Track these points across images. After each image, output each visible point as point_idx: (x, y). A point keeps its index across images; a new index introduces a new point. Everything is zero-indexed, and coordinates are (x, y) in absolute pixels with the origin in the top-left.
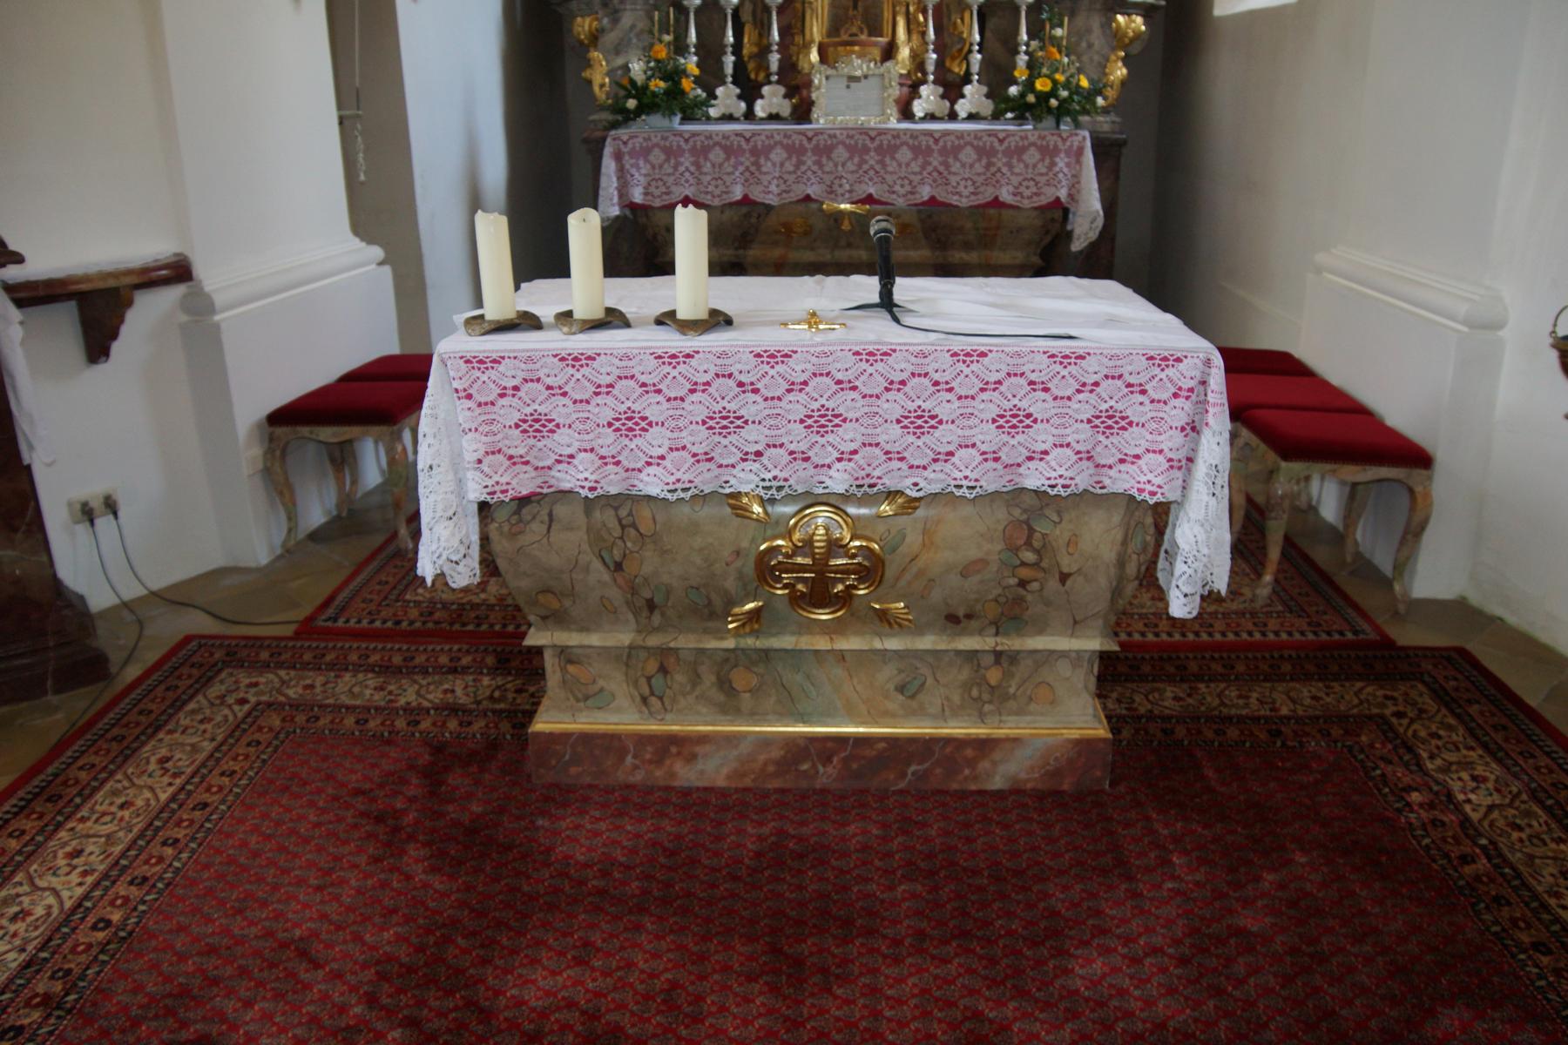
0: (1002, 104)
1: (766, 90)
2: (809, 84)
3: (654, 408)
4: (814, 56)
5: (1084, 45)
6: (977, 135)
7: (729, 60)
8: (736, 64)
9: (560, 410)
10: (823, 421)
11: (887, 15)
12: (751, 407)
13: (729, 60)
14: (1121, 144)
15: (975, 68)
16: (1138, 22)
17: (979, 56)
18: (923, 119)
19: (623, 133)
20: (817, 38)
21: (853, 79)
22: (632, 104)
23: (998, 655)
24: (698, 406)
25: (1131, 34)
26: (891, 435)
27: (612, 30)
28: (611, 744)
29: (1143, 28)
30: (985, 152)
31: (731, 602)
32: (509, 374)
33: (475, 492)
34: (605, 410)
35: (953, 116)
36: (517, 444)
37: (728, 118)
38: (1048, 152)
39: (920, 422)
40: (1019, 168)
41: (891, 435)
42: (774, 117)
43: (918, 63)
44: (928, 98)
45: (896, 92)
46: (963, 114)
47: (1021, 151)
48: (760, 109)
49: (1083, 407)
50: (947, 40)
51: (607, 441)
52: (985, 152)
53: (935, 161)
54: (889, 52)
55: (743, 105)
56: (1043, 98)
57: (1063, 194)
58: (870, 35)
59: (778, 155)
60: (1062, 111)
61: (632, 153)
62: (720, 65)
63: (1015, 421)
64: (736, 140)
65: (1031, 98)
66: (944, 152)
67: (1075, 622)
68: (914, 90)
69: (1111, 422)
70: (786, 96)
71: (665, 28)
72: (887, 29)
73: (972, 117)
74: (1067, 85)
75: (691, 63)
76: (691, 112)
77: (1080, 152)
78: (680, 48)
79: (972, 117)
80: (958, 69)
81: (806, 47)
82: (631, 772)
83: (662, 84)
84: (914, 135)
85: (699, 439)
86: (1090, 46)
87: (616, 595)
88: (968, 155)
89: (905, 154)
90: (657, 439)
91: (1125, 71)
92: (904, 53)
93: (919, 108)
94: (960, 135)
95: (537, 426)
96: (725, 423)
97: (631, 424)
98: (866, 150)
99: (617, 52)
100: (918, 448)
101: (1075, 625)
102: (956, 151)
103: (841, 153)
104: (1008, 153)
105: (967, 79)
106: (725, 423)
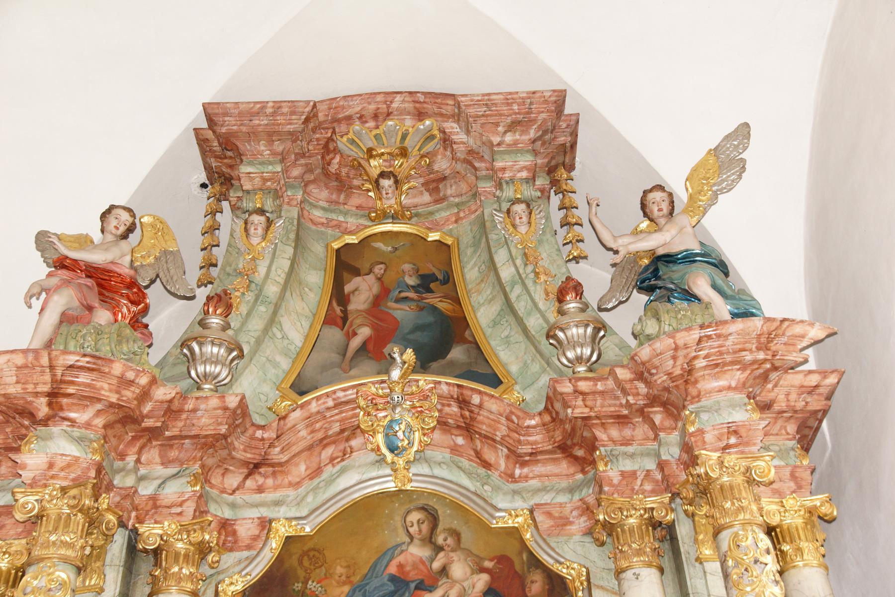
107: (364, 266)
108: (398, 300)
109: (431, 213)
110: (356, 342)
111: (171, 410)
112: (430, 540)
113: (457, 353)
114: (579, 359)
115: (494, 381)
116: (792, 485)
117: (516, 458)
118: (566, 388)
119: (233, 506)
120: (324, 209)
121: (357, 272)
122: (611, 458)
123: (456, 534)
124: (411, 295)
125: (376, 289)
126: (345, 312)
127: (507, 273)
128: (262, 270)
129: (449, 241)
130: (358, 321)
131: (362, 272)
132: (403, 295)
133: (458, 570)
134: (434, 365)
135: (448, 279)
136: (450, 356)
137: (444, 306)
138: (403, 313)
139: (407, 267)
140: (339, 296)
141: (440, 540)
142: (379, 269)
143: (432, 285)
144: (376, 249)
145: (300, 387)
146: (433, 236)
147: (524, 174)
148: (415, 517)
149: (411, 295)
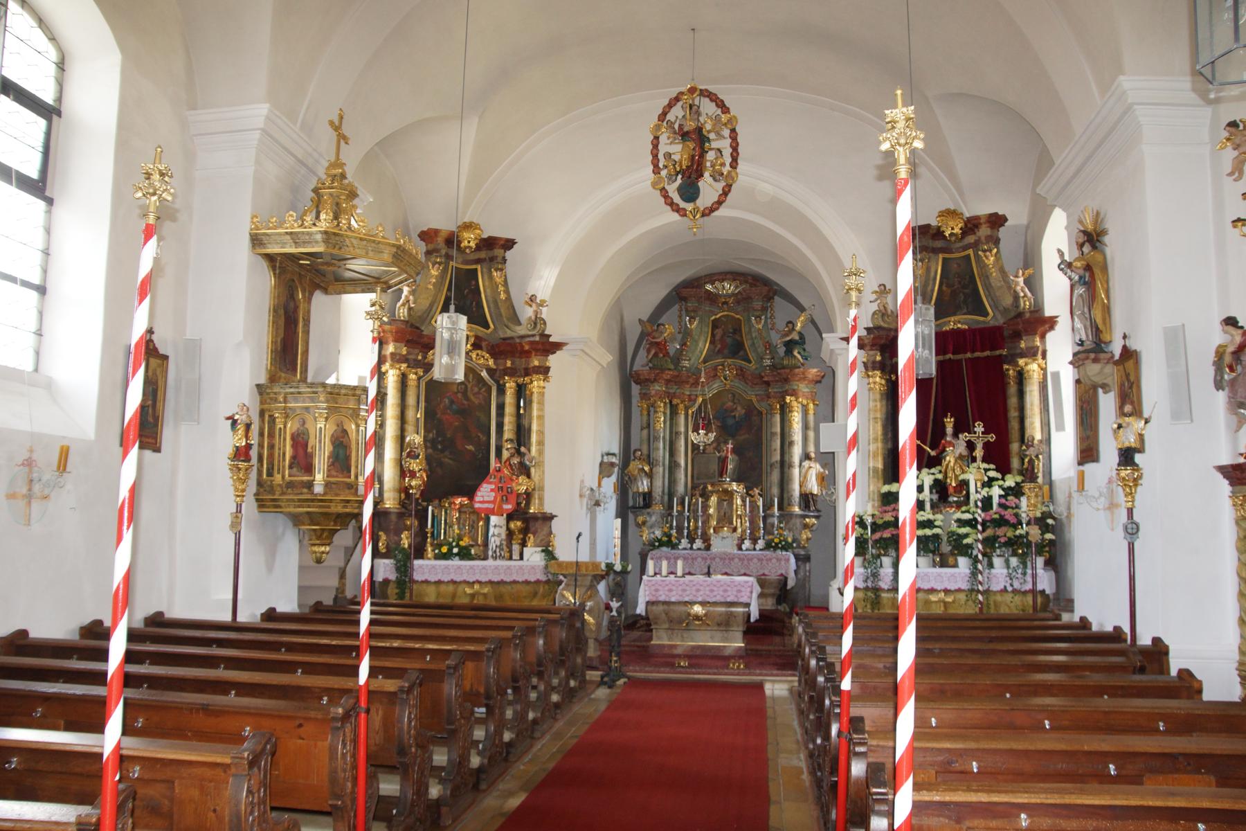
0: (769, 546)
1: (697, 541)
2: (710, 539)
3: (674, 588)
4: (712, 531)
6: (758, 555)
7: (686, 531)
8: (688, 533)
9: (660, 588)
10: (698, 590)
11: (735, 519)
12: (688, 588)
13: (686, 531)
15: (762, 535)
16: (814, 520)
18: (747, 550)
19: (654, 552)
21: (723, 538)
22: (657, 544)
24: (680, 588)
26: (708, 593)
28: (663, 646)
30: (760, 560)
31: (683, 621)
32: (653, 583)
33: (647, 599)
34: (667, 588)
35: (755, 549)
36: (654, 593)
37: (685, 549)
38: (779, 560)
39: (712, 591)
40: (770, 565)
41: (708, 593)
42: (699, 549)
44: (747, 544)
45: (736, 542)
46: (758, 549)
47: (770, 559)
48: (695, 547)
49: (735, 589)
51: (667, 593)
52: (760, 560)
53: (746, 562)
54: (735, 530)
55: (689, 545)
56: (777, 544)
57: (783, 572)
59: (699, 560)
60: (784, 548)
61: (657, 558)
62: (683, 533)
63: (725, 591)
64: (687, 556)
65: (773, 544)
66: (748, 560)
68: (742, 542)
69: (739, 591)
70: (704, 543)
71: (667, 523)
72: (735, 523)
73: (761, 550)
74: (784, 540)
75: (674, 532)
76: (674, 546)
77: (788, 560)
78: (671, 527)
79: (761, 550)
81: (709, 528)
82: (666, 651)
83: (666, 539)
84: (739, 555)
85: (680, 593)
87: (666, 619)
88: (755, 560)
89: (737, 560)
90: (674, 593)
92: (739, 530)
93: (744, 547)
94: (753, 555)
95: (657, 590)
96: (684, 590)
97: (670, 590)
98: (725, 559)
100: (712, 595)
101: (738, 626)
102: (751, 559)
103: (717, 560)
104: (767, 560)
105: (760, 539)
106: (684, 590)
108: (728, 337)
110: (717, 349)
111: (678, 376)
112: (733, 401)
113: (741, 353)
114: (767, 366)
115: (750, 362)
117: (753, 384)
118: (763, 374)
119: (690, 391)
121: (717, 328)
122: (773, 388)
123: (739, 400)
125: (722, 332)
127: (754, 335)
128: (694, 333)
129: (741, 318)
133: (739, 408)
135: (740, 330)
137: (739, 338)
139: (730, 326)
140: (713, 335)
141: (736, 401)
145: (705, 361)
146: (738, 316)
148: (730, 396)
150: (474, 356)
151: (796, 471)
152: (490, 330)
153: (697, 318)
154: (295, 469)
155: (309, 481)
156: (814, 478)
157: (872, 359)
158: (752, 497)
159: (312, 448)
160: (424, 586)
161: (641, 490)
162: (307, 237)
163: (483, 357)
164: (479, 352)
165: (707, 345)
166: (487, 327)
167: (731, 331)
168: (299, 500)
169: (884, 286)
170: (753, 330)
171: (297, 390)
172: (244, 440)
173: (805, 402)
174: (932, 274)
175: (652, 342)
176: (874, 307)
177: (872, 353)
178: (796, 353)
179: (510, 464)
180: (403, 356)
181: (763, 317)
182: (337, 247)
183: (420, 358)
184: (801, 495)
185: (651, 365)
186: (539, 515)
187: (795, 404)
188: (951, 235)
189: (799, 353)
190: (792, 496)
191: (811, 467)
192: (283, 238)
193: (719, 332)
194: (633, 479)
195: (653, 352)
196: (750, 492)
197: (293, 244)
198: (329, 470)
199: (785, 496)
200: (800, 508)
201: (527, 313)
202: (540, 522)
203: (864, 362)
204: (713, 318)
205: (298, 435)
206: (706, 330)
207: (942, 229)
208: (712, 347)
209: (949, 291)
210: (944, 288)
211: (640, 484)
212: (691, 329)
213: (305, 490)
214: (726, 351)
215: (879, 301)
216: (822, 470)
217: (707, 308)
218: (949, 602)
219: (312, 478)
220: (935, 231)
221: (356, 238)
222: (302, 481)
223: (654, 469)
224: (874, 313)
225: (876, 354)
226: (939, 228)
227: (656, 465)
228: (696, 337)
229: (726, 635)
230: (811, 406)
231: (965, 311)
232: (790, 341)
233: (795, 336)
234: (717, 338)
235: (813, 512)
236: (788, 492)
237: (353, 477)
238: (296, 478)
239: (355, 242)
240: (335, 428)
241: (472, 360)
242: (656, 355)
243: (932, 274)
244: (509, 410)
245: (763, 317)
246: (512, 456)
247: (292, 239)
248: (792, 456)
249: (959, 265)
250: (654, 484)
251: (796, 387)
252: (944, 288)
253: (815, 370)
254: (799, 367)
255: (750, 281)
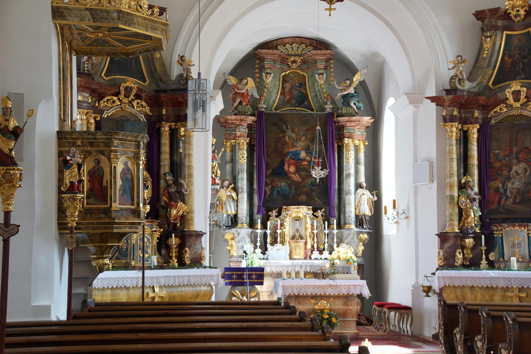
5: (352, 241)
14: (363, 265)
17: (327, 244)
20: (288, 240)
23: (343, 320)
25: (364, 239)
27: (238, 237)
29: (367, 237)
43: (313, 247)
46: (323, 258)
50: (319, 240)
58: (301, 239)
67: (353, 316)
80: (322, 247)
86: (354, 242)
91: (363, 247)
93: (313, 257)
99: (239, 242)
105: (324, 250)
107: (288, 80)
108: (295, 90)
109: (302, 67)
110: (286, 99)
113: (306, 103)
115: (313, 110)
116: (362, 138)
120: (280, 65)
121: (286, 82)
124: (298, 88)
125: (290, 86)
126: (284, 92)
127: (317, 89)
130: (287, 94)
131: (288, 82)
132: (296, 88)
134: (302, 105)
135: (305, 85)
136: (305, 104)
137: (304, 91)
138: (296, 92)
139: (297, 81)
140: (283, 88)
142: (291, 81)
143: (302, 86)
144: (291, 76)
147: (323, 68)
149: (297, 88)
150: (135, 103)
151: (352, 197)
152: (146, 83)
153: (272, 75)
154: (92, 199)
155: (105, 208)
156: (366, 202)
157: (450, 113)
158: (317, 217)
159: (107, 182)
160: (119, 291)
161: (229, 213)
162: (105, 14)
163: (142, 105)
164: (139, 101)
165: (279, 96)
166: (145, 81)
167: (297, 85)
168: (98, 223)
169: (461, 56)
170: (316, 85)
171: (94, 137)
172: (78, 177)
173: (357, 142)
174: (497, 47)
175: (236, 92)
176: (452, 73)
177: (450, 109)
178: (352, 105)
179: (168, 191)
180: (89, 103)
181: (325, 75)
182: (128, 24)
183: (97, 105)
184: (357, 216)
185: (236, 112)
186: (194, 233)
187: (351, 144)
188: (516, 16)
189: (354, 104)
190: (349, 216)
191: (364, 194)
192: (83, 13)
193: (288, 86)
194: (222, 204)
195: (238, 101)
196: (315, 214)
197: (91, 18)
198: (120, 200)
199: (342, 217)
200: (356, 226)
201: (176, 71)
202: (193, 238)
203: (443, 116)
204: (284, 74)
205: (94, 172)
206: (277, 83)
207: (509, 11)
208: (282, 97)
209: (510, 61)
210: (506, 59)
211: (228, 208)
212: (267, 84)
213: (102, 216)
214: (293, 102)
215: (456, 69)
216: (371, 197)
217: (279, 66)
218: (523, 297)
219: (109, 206)
220: (503, 13)
221: (141, 17)
222: (100, 208)
223: (240, 196)
224: (452, 78)
225: (454, 110)
226: (507, 10)
227: (242, 192)
228: (271, 89)
229: (343, 324)
230: (362, 147)
231: (523, 76)
232: (348, 94)
233: (351, 90)
234: (287, 90)
235: (365, 229)
236: (345, 213)
237: (135, 204)
238: (93, 206)
239: (140, 20)
240: (123, 167)
241: (133, 107)
242: (240, 103)
243: (497, 47)
244: (166, 148)
245: (325, 75)
246: (169, 186)
247: (91, 14)
248: (349, 186)
249: (520, 40)
250: (239, 208)
251: (353, 131)
252: (506, 59)
253: (369, 118)
254: (355, 116)
255: (314, 45)
